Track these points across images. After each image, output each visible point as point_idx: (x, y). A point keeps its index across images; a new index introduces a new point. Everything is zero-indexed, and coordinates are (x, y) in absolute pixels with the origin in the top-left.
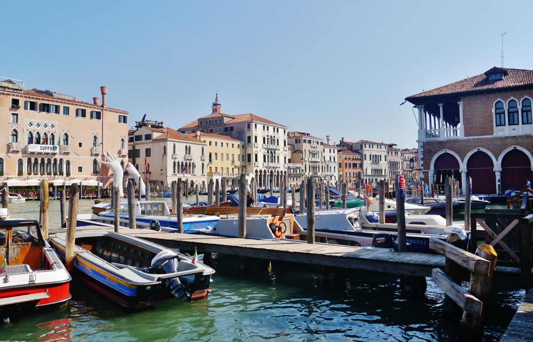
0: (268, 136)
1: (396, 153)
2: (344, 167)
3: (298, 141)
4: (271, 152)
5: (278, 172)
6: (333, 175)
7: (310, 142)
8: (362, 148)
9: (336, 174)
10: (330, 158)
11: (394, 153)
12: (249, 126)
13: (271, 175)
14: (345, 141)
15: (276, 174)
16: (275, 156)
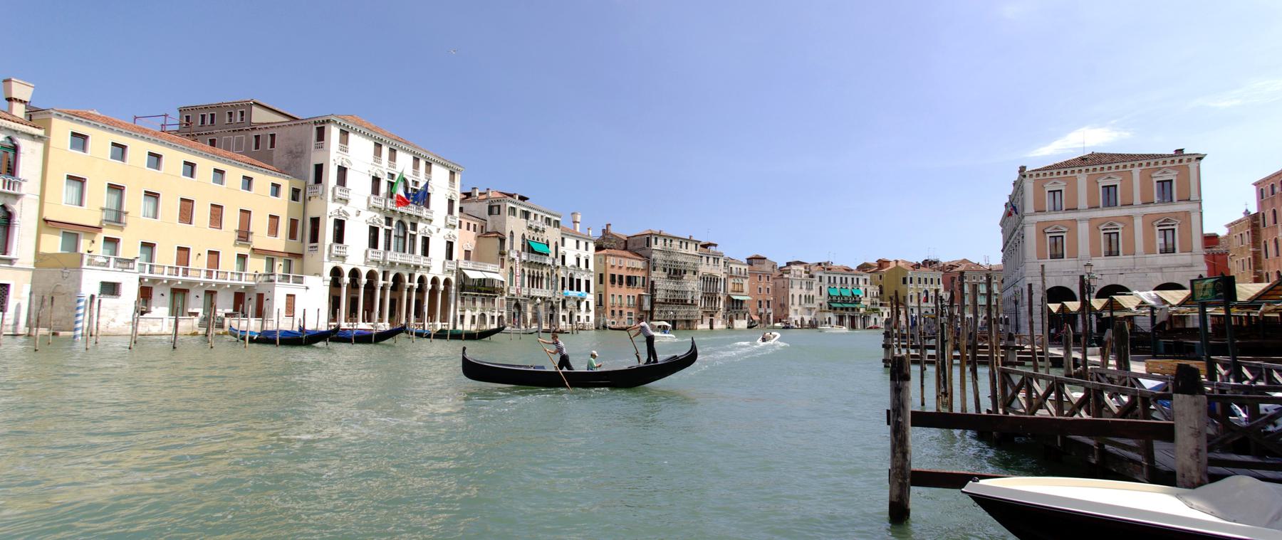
0: (392, 176)
1: (716, 259)
2: (609, 283)
3: (496, 209)
4: (401, 223)
5: (422, 280)
6: (583, 299)
7: (526, 215)
8: (648, 244)
9: (591, 298)
10: (578, 259)
11: (711, 260)
12: (321, 135)
13: (418, 291)
14: (612, 230)
15: (416, 285)
16: (413, 237)
